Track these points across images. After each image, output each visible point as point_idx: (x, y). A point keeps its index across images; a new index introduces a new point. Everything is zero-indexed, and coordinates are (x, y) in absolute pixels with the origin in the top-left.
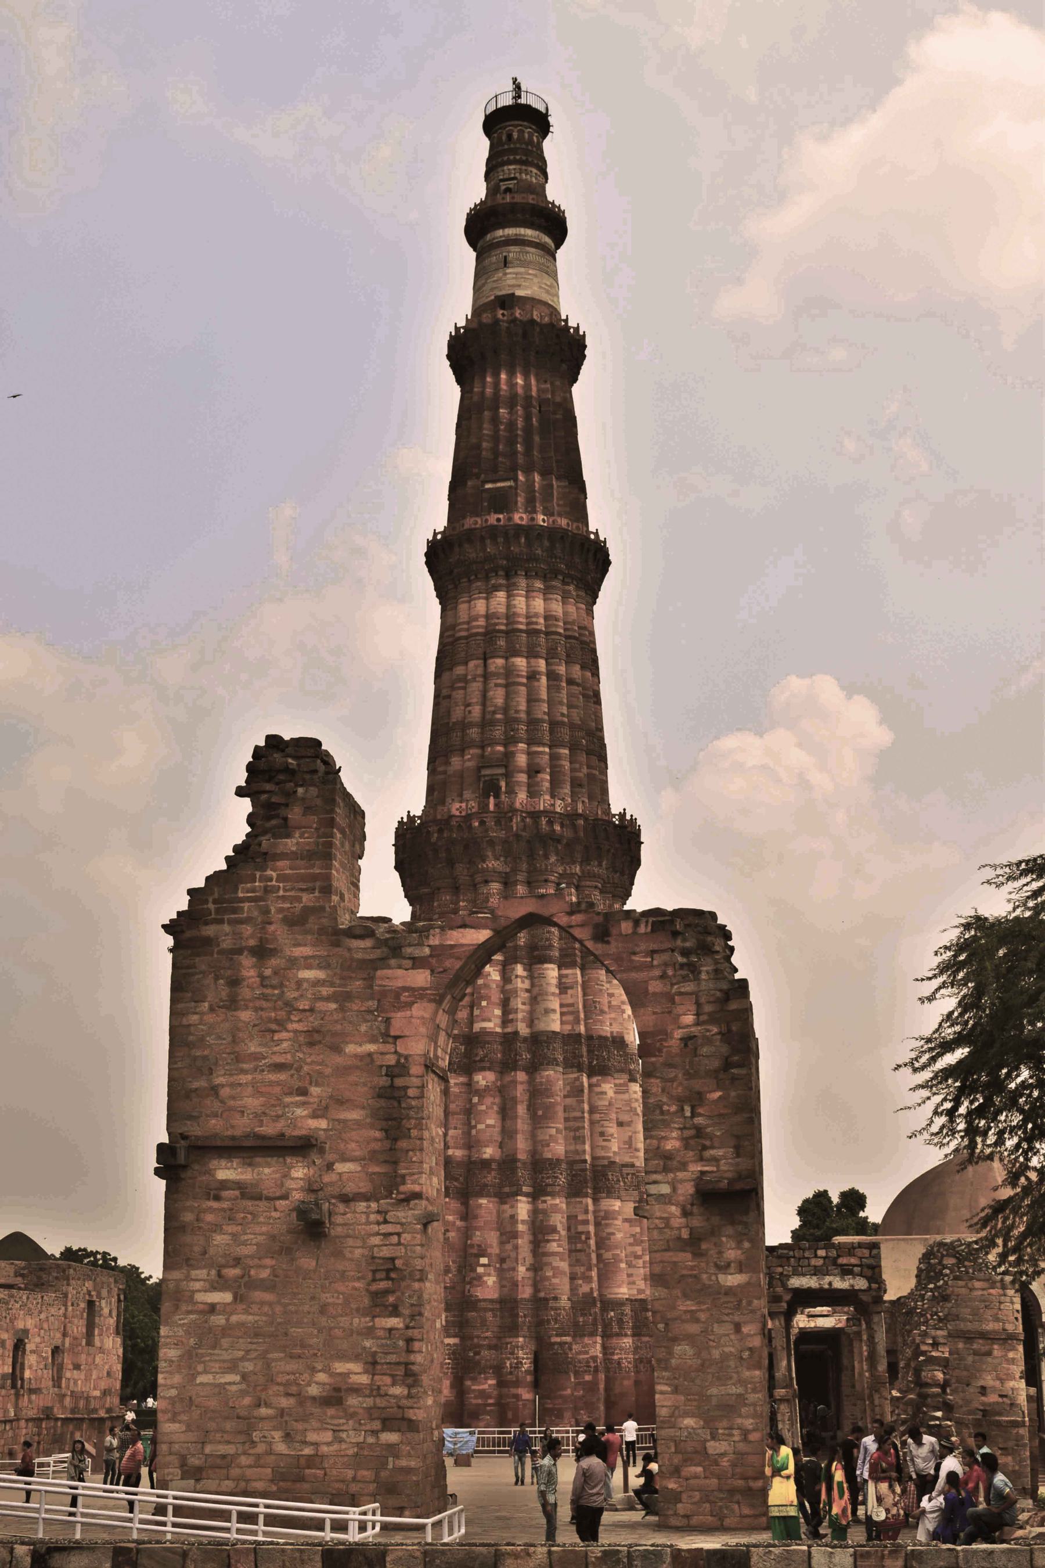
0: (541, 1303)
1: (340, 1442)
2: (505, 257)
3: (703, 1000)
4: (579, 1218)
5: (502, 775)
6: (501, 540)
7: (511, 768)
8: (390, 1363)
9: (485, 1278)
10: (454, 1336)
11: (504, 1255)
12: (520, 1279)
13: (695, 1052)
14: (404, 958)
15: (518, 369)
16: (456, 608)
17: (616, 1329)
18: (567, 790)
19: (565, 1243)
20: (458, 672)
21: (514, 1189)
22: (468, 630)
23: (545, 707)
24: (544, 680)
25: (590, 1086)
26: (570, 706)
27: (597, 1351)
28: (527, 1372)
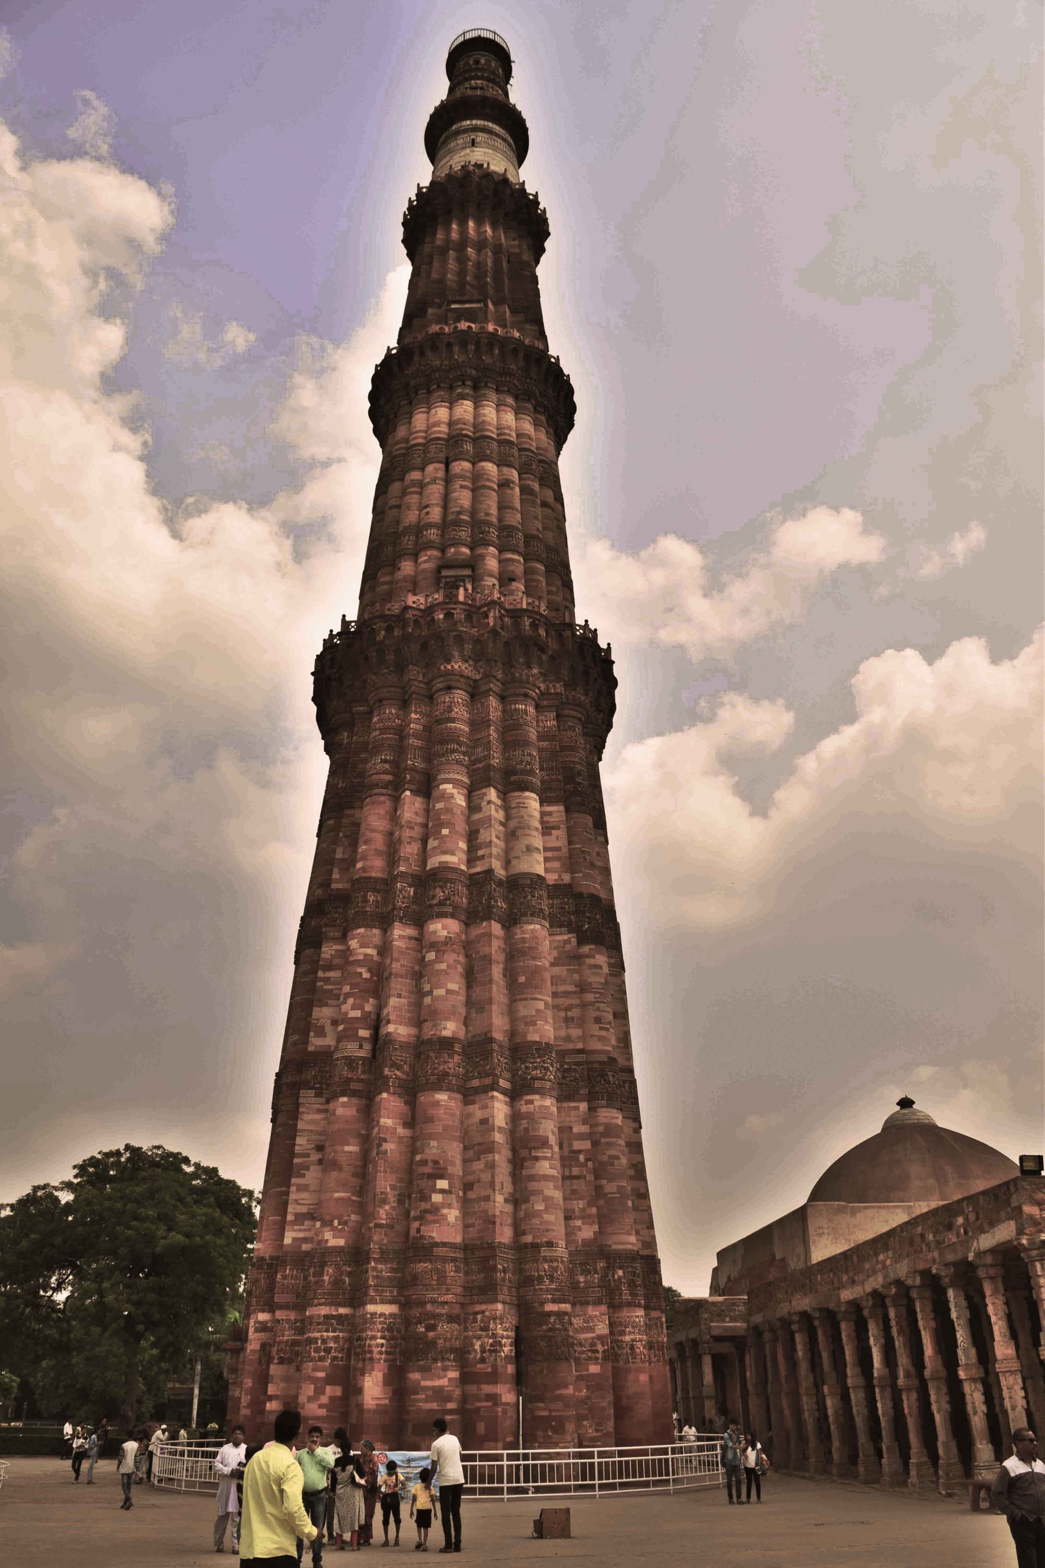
0: (526, 1251)
2: (473, 140)
4: (575, 1130)
5: (469, 576)
9: (445, 1211)
10: (391, 1302)
12: (498, 1213)
16: (410, 423)
17: (626, 1297)
19: (557, 1163)
20: (412, 477)
21: (488, 1081)
22: (425, 438)
23: (519, 516)
24: (517, 490)
26: (544, 529)
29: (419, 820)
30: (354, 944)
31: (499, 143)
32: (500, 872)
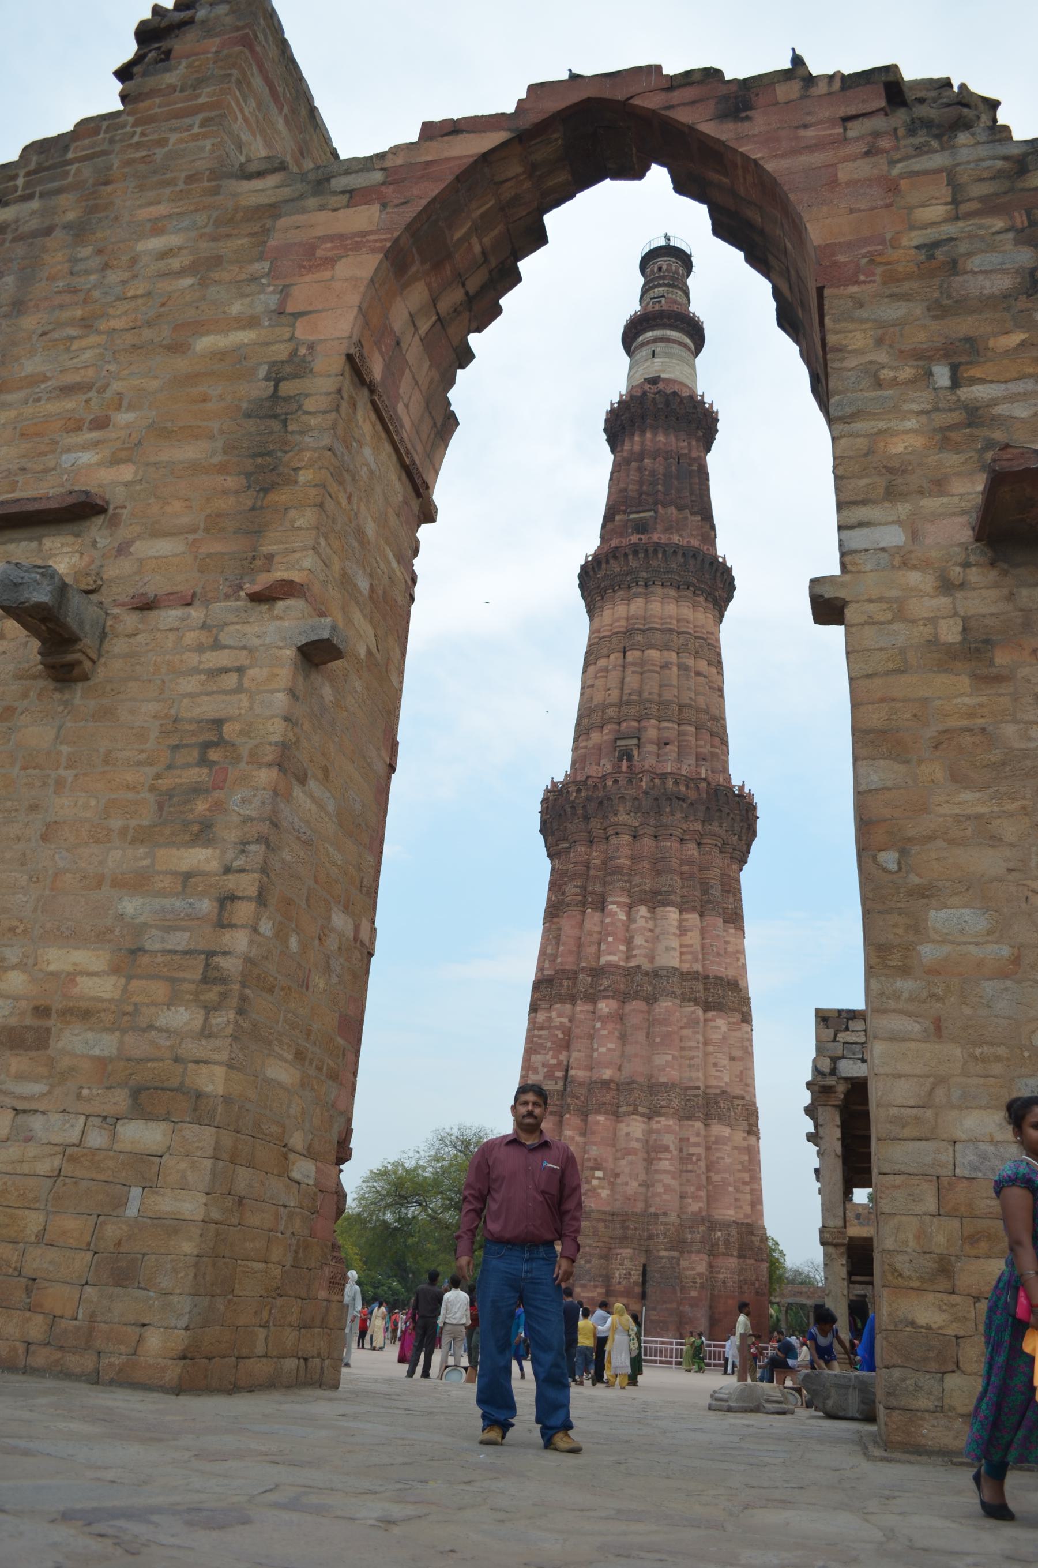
1: (28, 1140)
3: (965, 178)
4: (691, 1140)
6: (641, 555)
7: (643, 740)
8: (174, 952)
9: (600, 1191)
11: (618, 1170)
13: (953, 267)
14: (334, 193)
15: (660, 430)
18: (692, 761)
23: (675, 692)
24: (675, 669)
25: (706, 1020)
27: (702, 1267)
28: (635, 1283)
29: (597, 929)
30: (554, 1014)
31: (676, 349)
32: (647, 966)
